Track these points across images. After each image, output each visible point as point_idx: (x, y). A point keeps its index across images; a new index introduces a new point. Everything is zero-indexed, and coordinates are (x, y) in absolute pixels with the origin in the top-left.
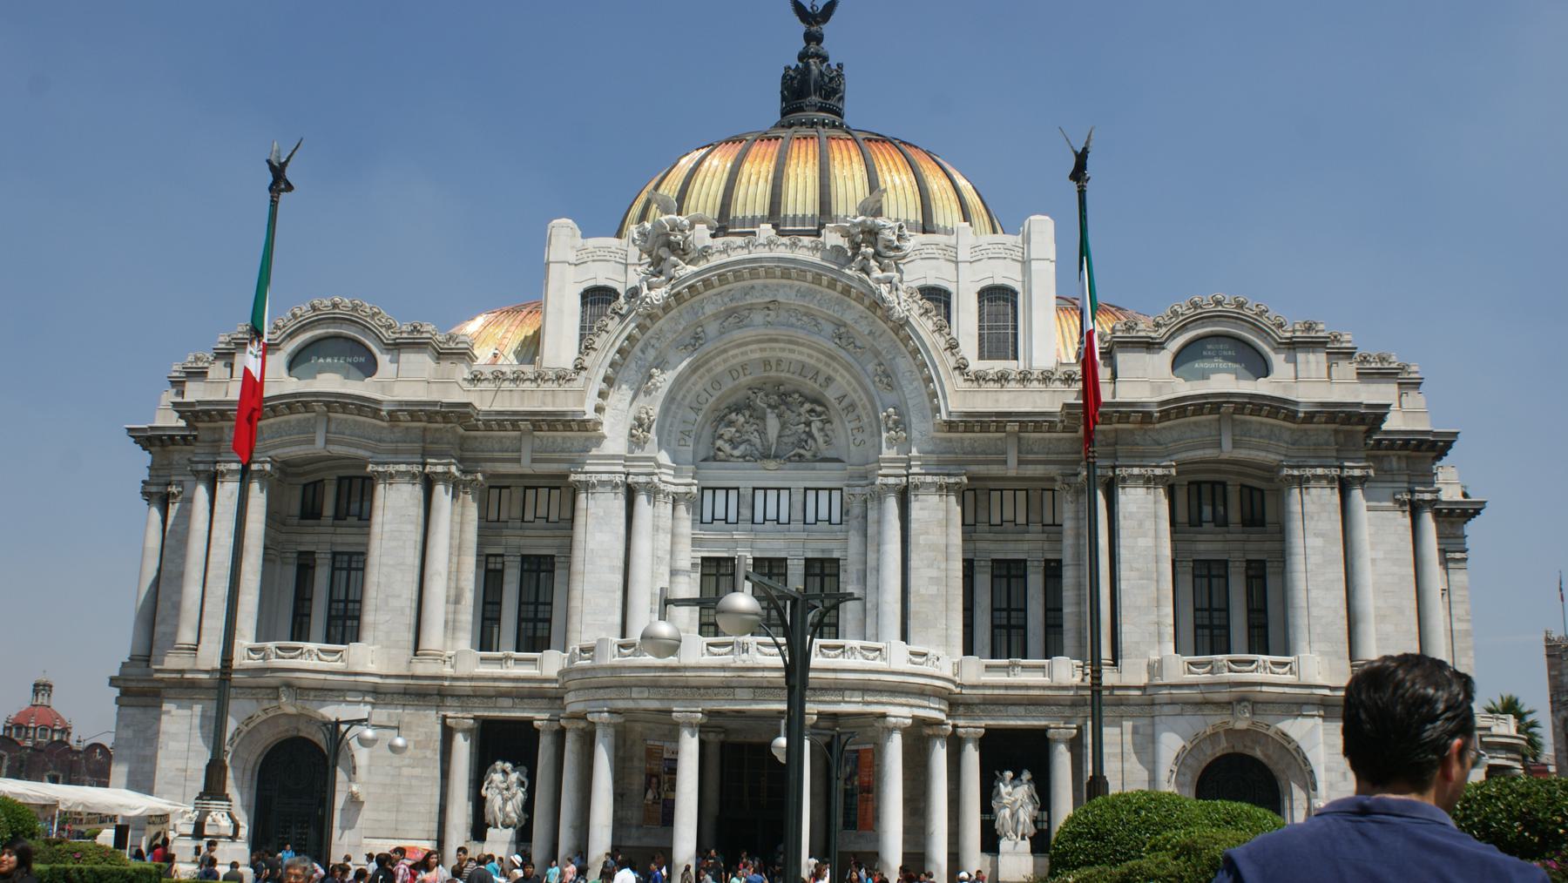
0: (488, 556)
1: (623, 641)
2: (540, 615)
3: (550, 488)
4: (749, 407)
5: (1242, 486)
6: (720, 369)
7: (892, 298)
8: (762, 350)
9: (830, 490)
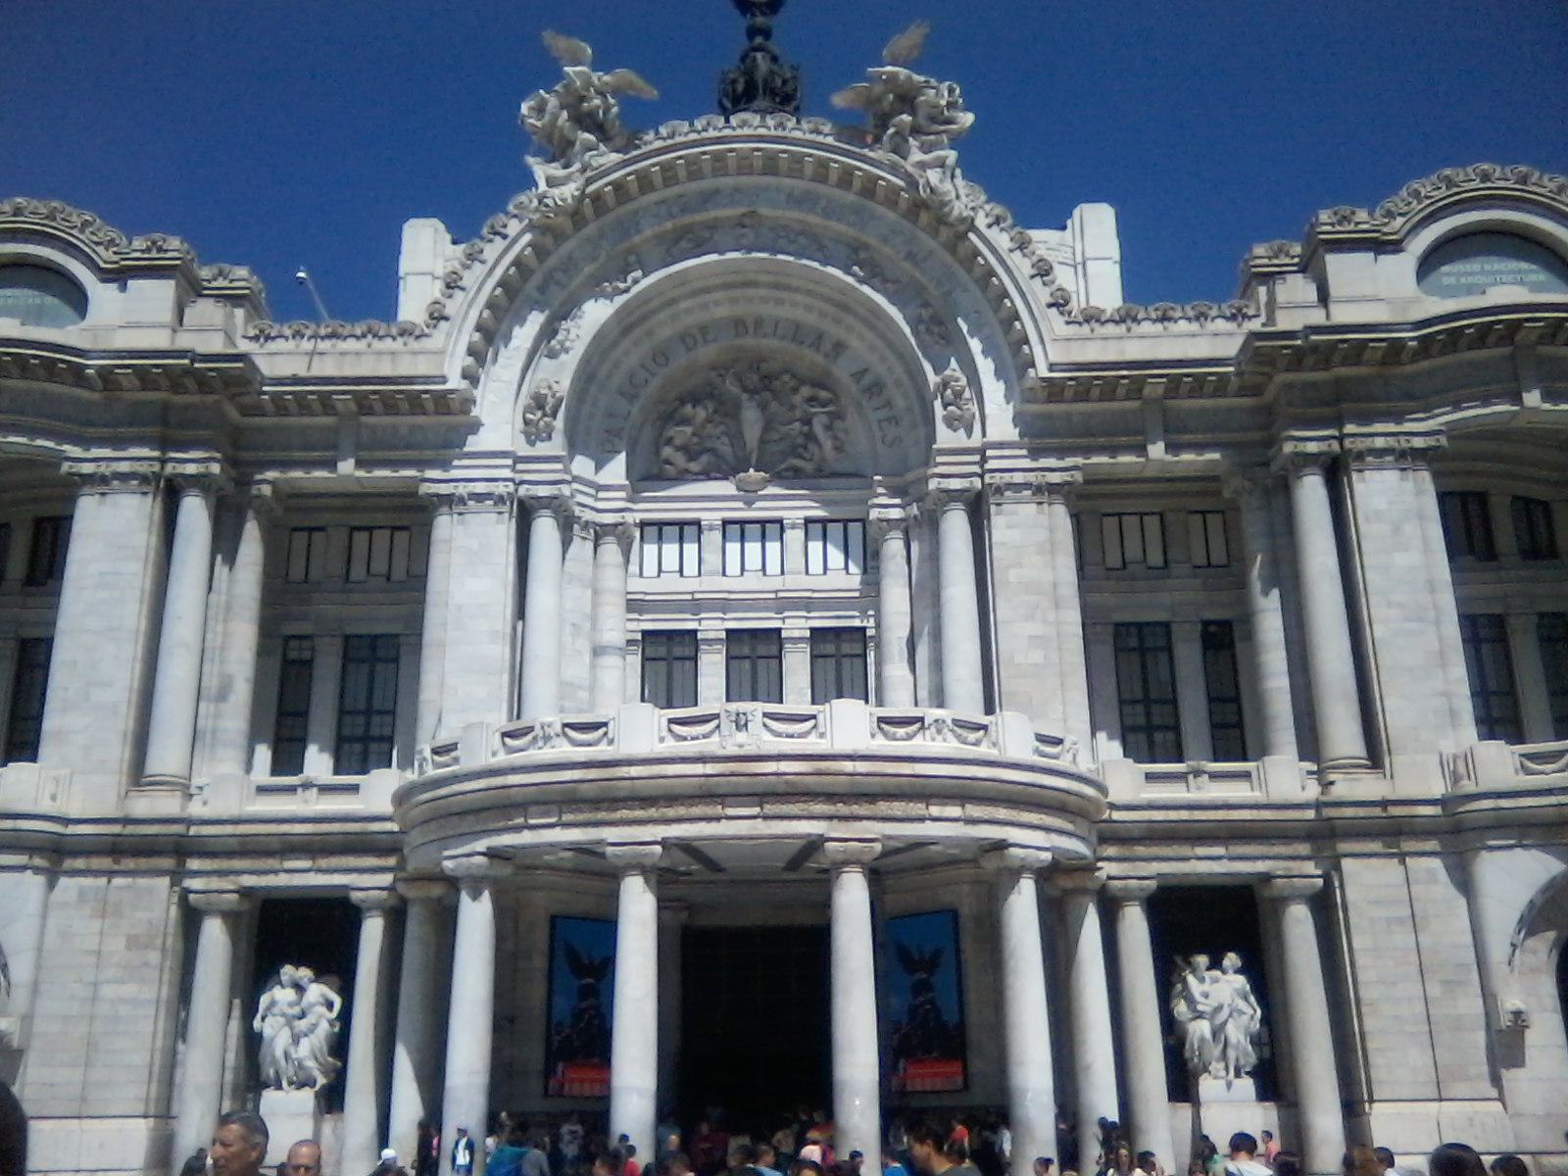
0: (288, 639)
1: (511, 727)
2: (375, 731)
3: (395, 529)
4: (711, 396)
5: (1516, 498)
6: (667, 332)
7: (947, 186)
8: (733, 301)
9: (846, 522)
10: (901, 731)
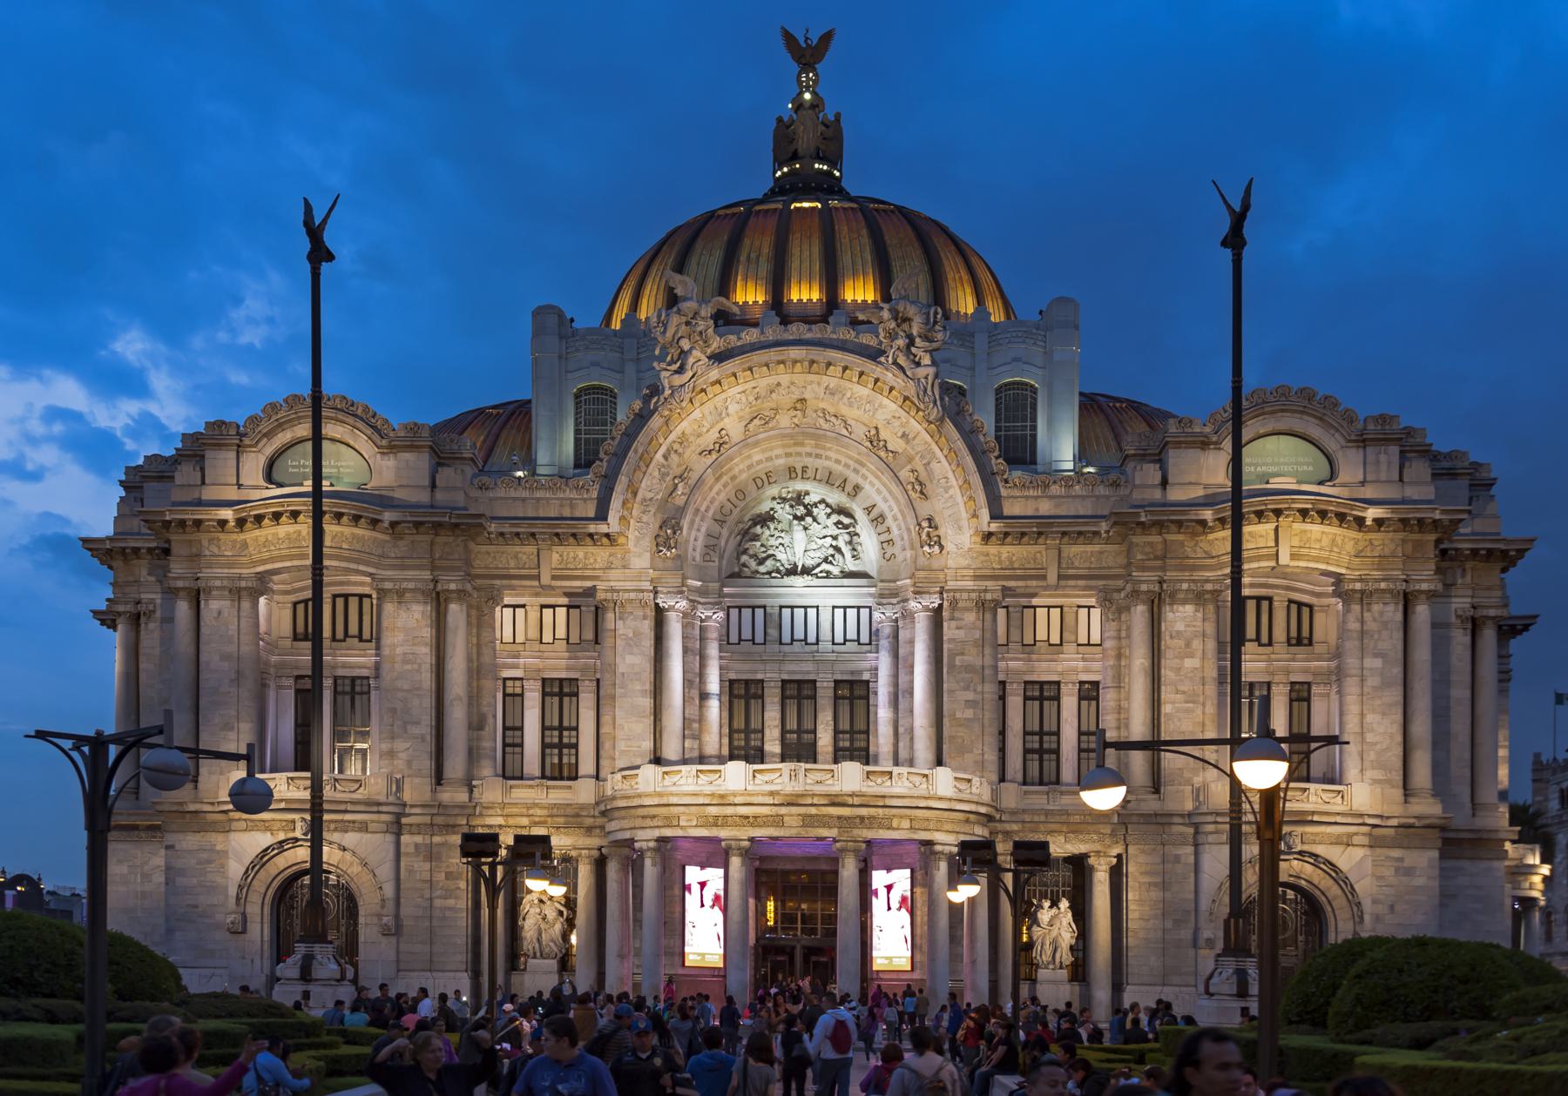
4: (772, 519)
5: (1291, 601)
10: (879, 781)
